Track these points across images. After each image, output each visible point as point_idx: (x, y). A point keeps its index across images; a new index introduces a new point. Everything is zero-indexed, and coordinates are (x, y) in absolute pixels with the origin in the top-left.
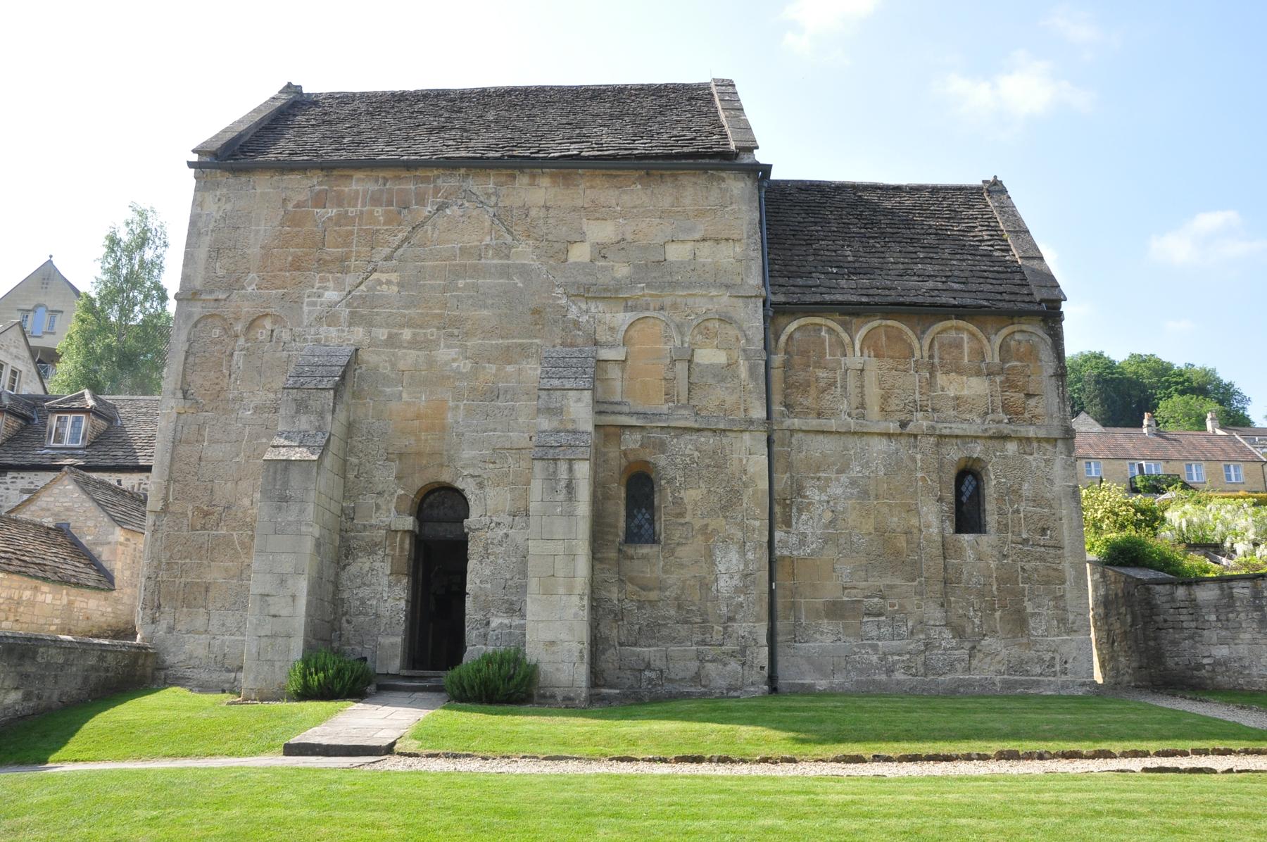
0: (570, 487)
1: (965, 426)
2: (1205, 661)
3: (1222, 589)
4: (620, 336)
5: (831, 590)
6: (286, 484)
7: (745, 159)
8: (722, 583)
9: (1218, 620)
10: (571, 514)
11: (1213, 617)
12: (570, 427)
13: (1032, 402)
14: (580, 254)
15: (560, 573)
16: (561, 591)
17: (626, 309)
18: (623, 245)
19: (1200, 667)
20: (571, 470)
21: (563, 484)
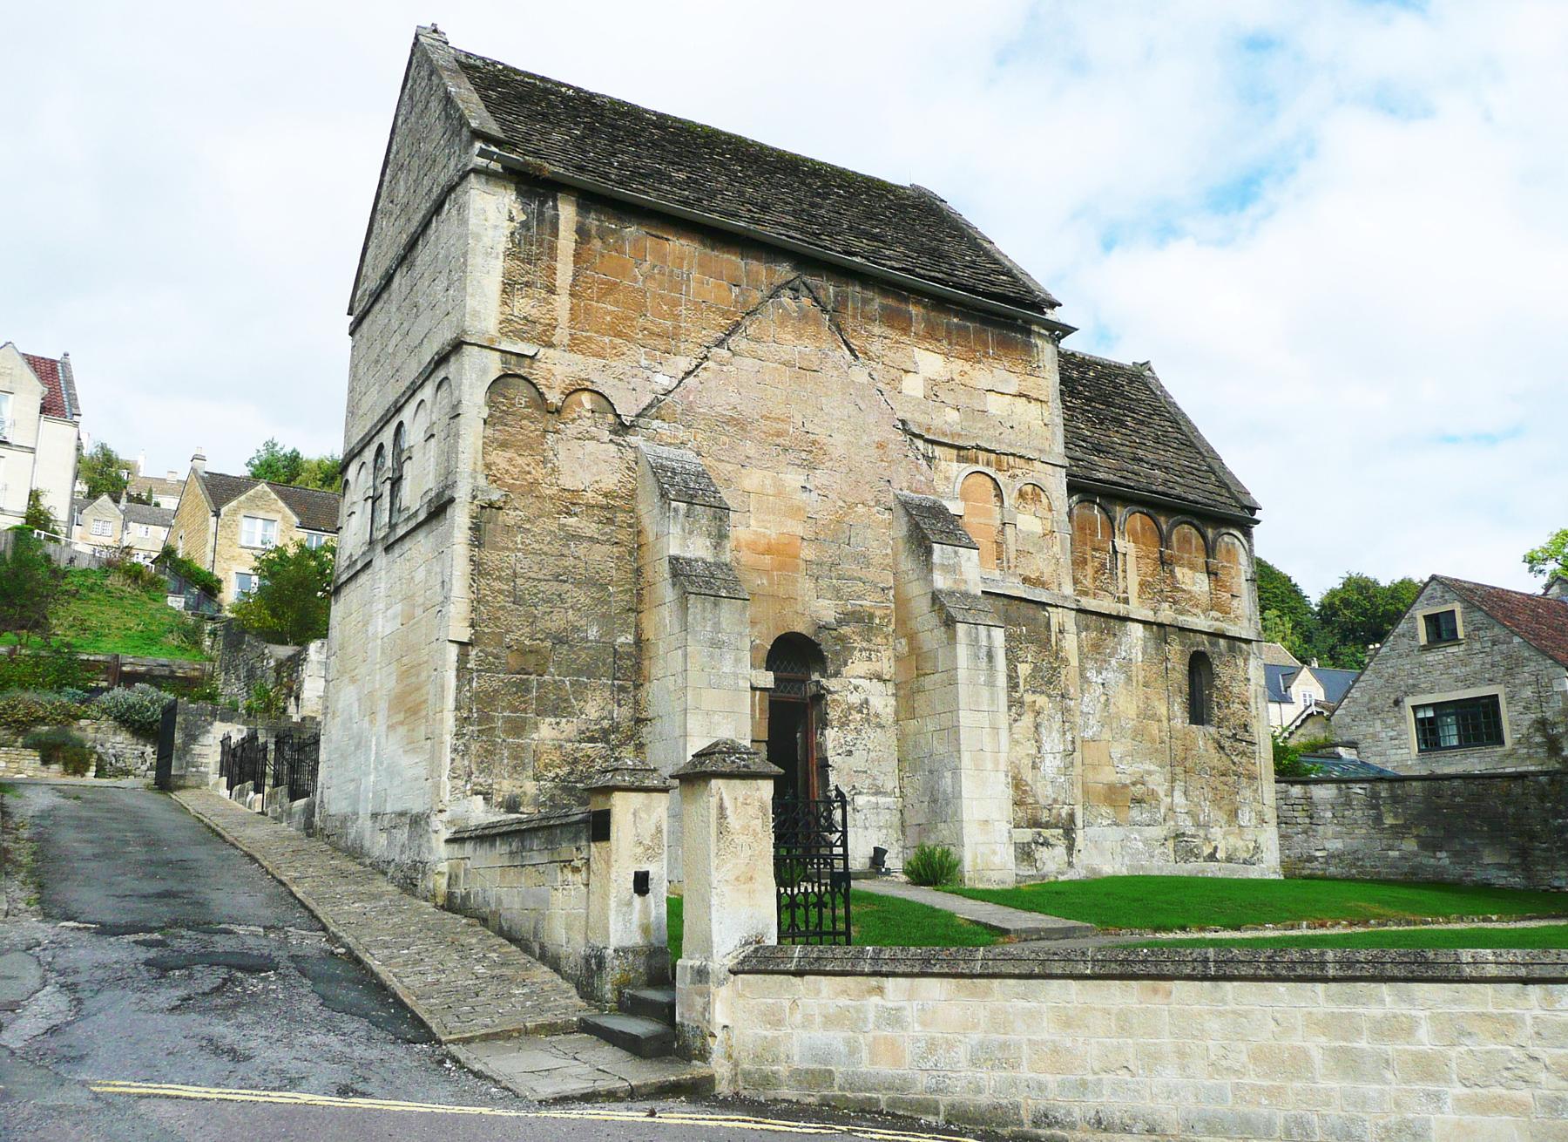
0: (990, 656)
1: (1195, 619)
2: (1318, 854)
3: (1340, 789)
4: (957, 489)
5: (1108, 776)
6: (717, 625)
7: (1051, 315)
8: (1048, 763)
9: (1334, 816)
10: (991, 683)
11: (1329, 814)
12: (963, 588)
13: (1235, 602)
14: (913, 386)
15: (988, 748)
16: (989, 766)
17: (960, 459)
18: (952, 385)
19: (1312, 859)
20: (989, 636)
21: (984, 651)
